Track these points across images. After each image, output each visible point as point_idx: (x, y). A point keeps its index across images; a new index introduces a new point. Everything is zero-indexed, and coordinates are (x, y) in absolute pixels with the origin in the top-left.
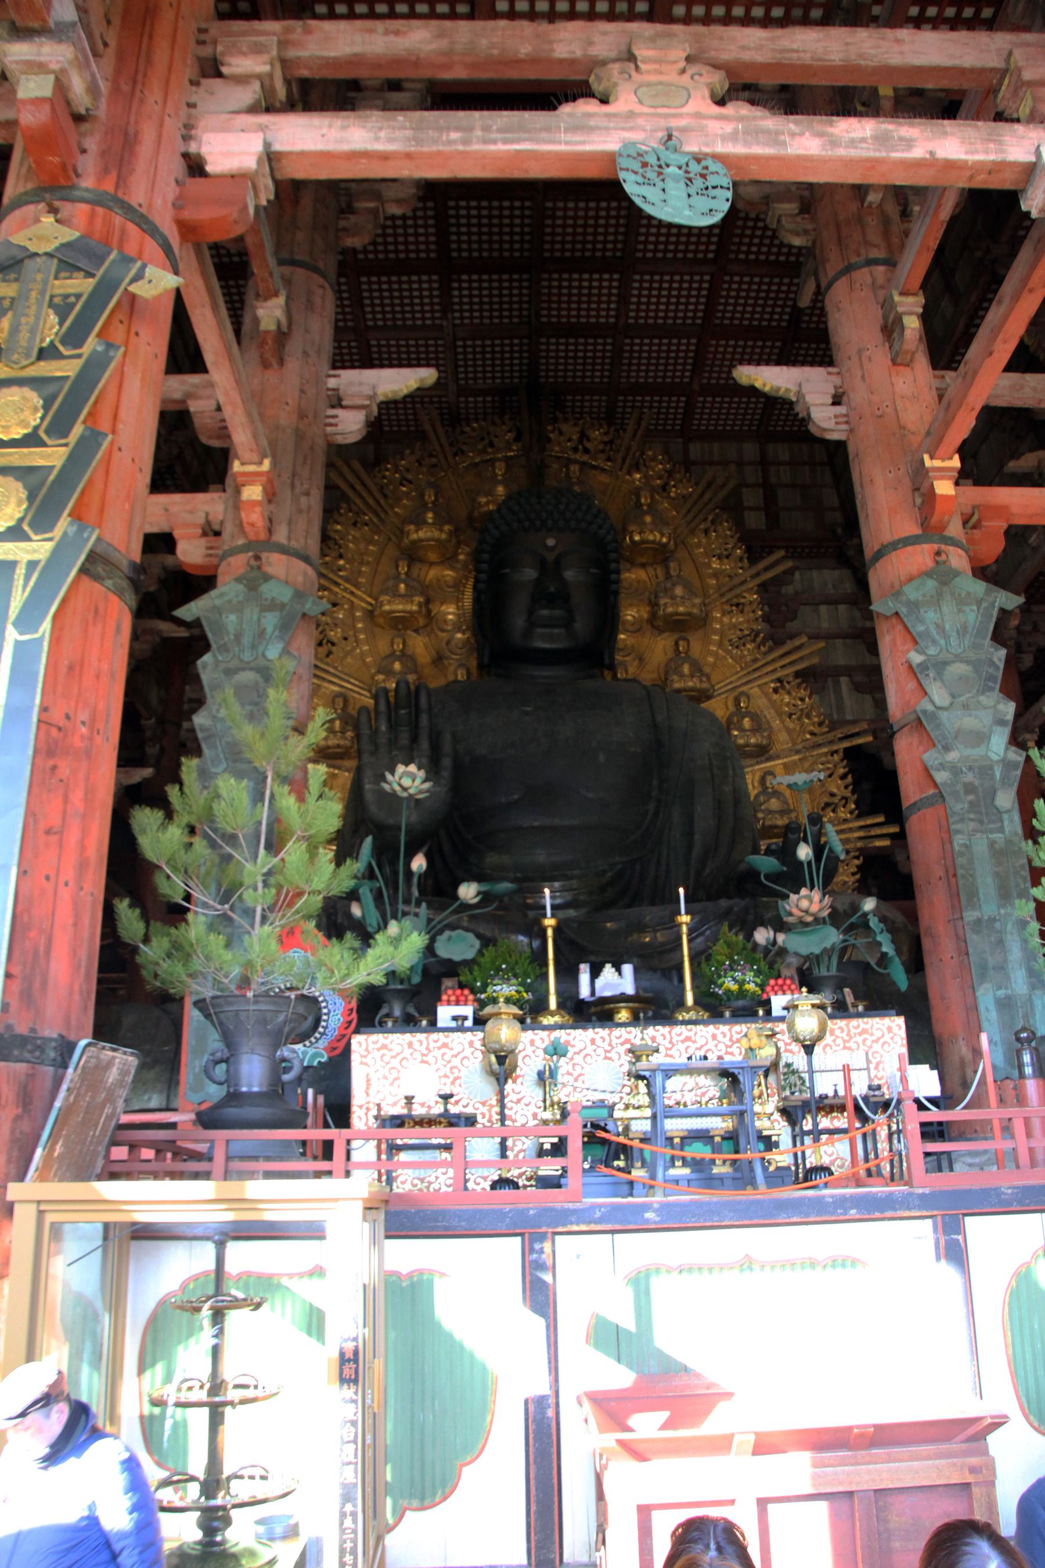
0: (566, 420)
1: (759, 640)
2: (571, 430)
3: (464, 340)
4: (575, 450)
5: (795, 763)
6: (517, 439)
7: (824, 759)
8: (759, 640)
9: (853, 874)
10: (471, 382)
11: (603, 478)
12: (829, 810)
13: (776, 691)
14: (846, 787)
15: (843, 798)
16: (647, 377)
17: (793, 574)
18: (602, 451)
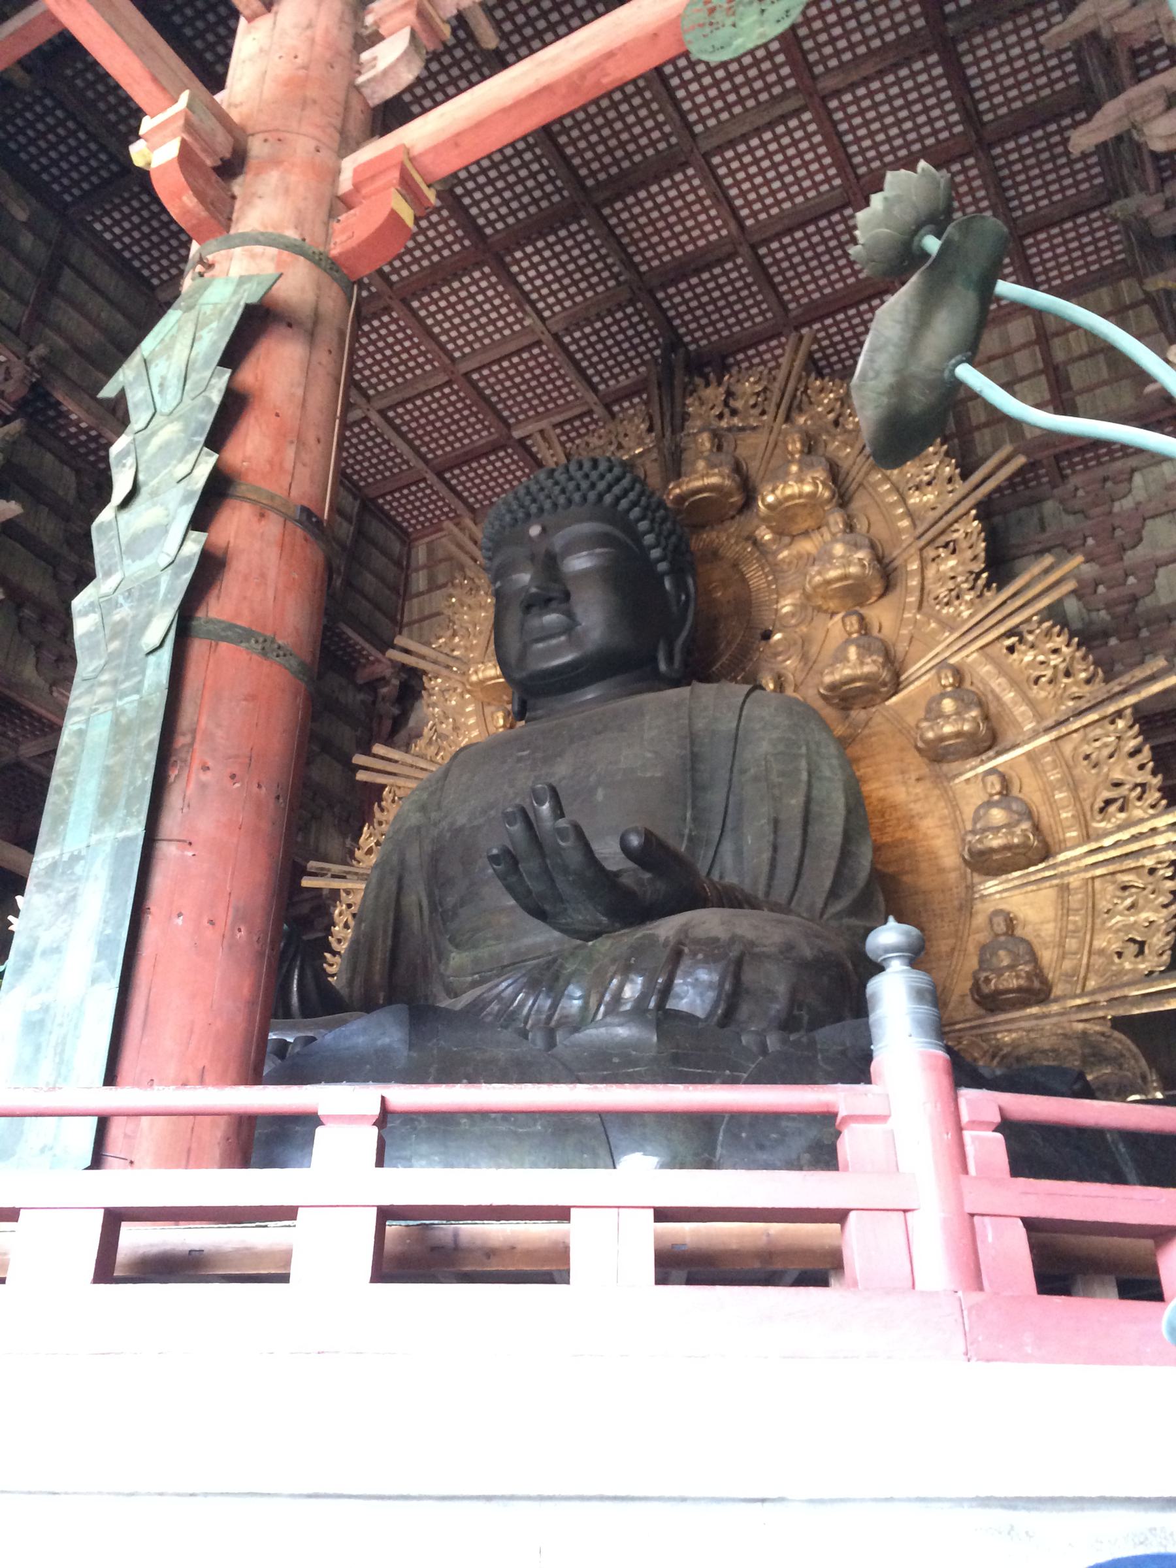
0: (707, 384)
1: (981, 582)
2: (714, 393)
3: (568, 331)
4: (721, 416)
5: (1045, 749)
6: (650, 430)
7: (1098, 731)
8: (981, 582)
9: (1165, 906)
10: (612, 382)
11: (751, 439)
12: (1113, 808)
13: (1011, 649)
14: (1141, 767)
15: (1136, 785)
16: (819, 289)
17: (1130, 480)
18: (754, 406)
